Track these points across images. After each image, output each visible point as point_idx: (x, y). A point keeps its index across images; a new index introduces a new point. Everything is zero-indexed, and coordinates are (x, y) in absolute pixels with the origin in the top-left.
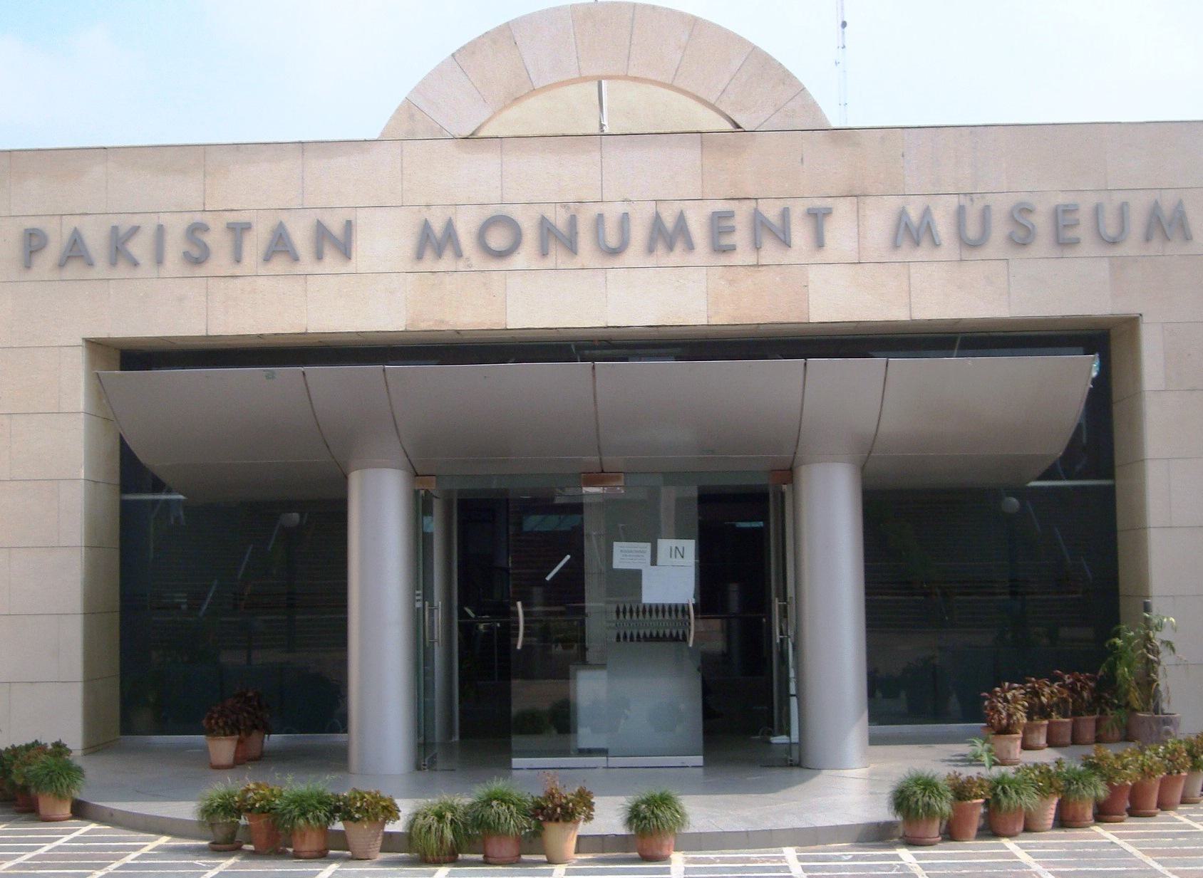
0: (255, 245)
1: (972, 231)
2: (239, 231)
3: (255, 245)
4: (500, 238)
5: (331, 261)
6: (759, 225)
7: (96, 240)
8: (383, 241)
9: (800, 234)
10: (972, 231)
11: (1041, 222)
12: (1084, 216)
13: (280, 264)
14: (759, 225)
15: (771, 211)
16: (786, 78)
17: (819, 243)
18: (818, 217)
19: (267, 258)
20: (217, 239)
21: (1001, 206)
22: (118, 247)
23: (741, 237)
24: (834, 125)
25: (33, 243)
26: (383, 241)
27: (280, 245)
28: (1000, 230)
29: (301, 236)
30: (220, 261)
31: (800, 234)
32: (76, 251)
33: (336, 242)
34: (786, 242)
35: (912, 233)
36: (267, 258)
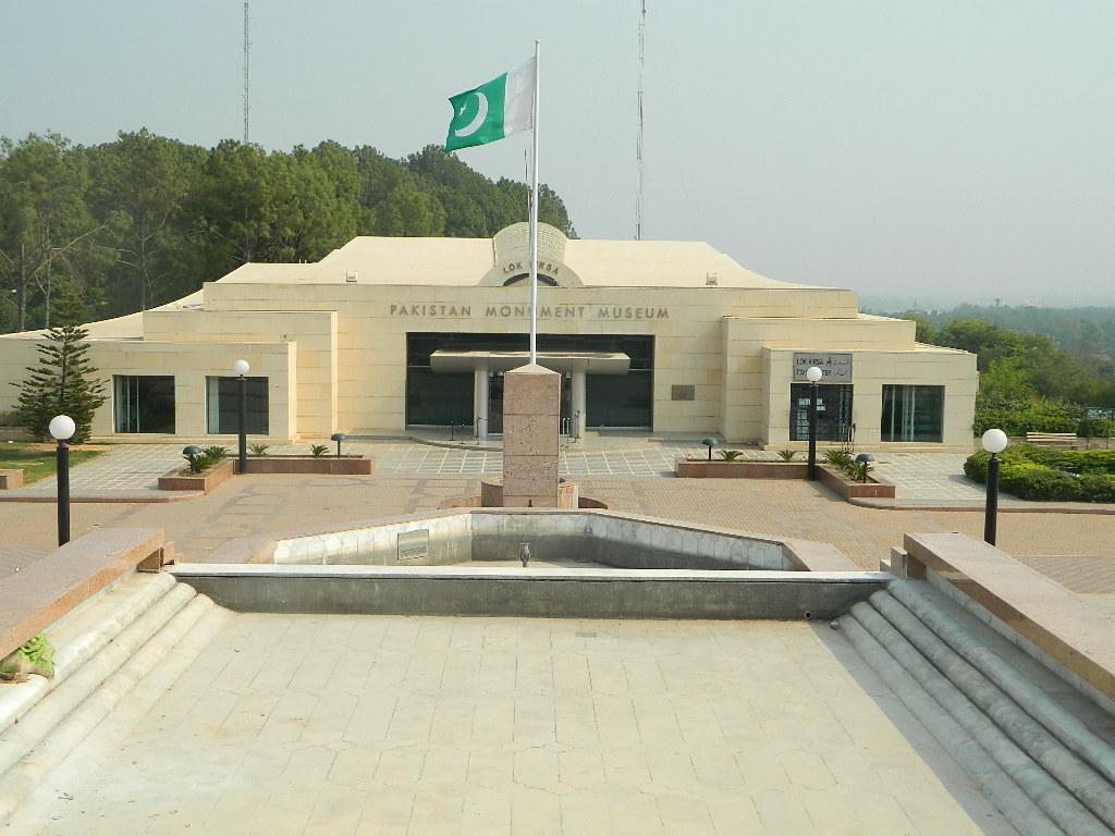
0: (447, 311)
1: (617, 314)
2: (443, 307)
3: (447, 311)
4: (506, 312)
5: (466, 316)
6: (567, 310)
7: (409, 310)
8: (478, 312)
9: (577, 312)
10: (617, 314)
11: (634, 314)
12: (644, 311)
13: (453, 316)
14: (567, 310)
15: (570, 307)
16: (575, 275)
17: (581, 314)
18: (581, 309)
19: (450, 314)
20: (438, 310)
21: (624, 308)
22: (414, 311)
23: (563, 314)
24: (586, 283)
25: (393, 308)
26: (478, 312)
27: (453, 311)
28: (624, 313)
29: (458, 311)
30: (439, 315)
31: (577, 312)
32: (404, 310)
33: (466, 311)
34: (573, 314)
35: (603, 314)
36: (450, 314)
